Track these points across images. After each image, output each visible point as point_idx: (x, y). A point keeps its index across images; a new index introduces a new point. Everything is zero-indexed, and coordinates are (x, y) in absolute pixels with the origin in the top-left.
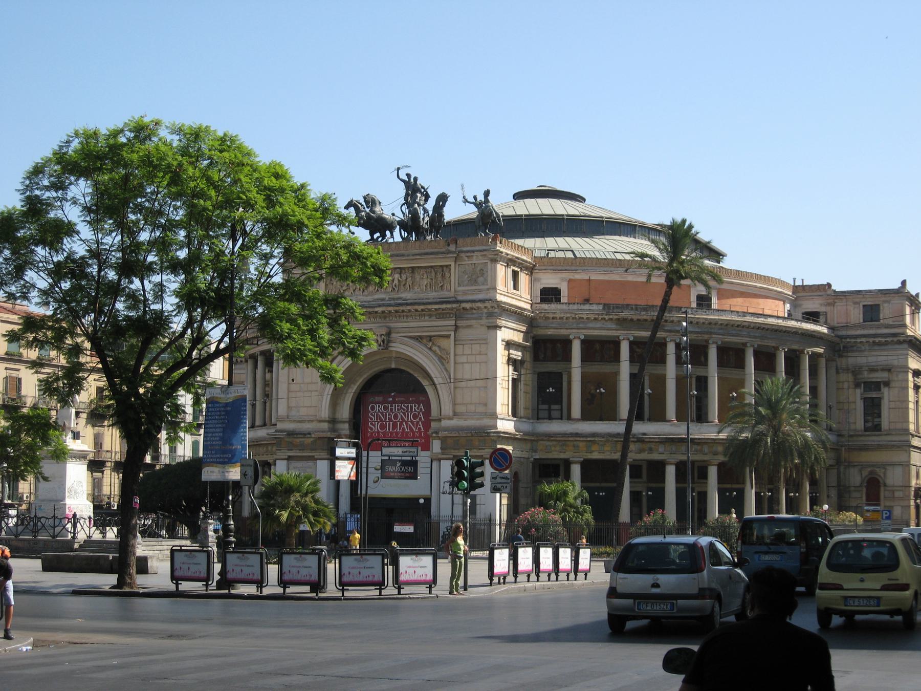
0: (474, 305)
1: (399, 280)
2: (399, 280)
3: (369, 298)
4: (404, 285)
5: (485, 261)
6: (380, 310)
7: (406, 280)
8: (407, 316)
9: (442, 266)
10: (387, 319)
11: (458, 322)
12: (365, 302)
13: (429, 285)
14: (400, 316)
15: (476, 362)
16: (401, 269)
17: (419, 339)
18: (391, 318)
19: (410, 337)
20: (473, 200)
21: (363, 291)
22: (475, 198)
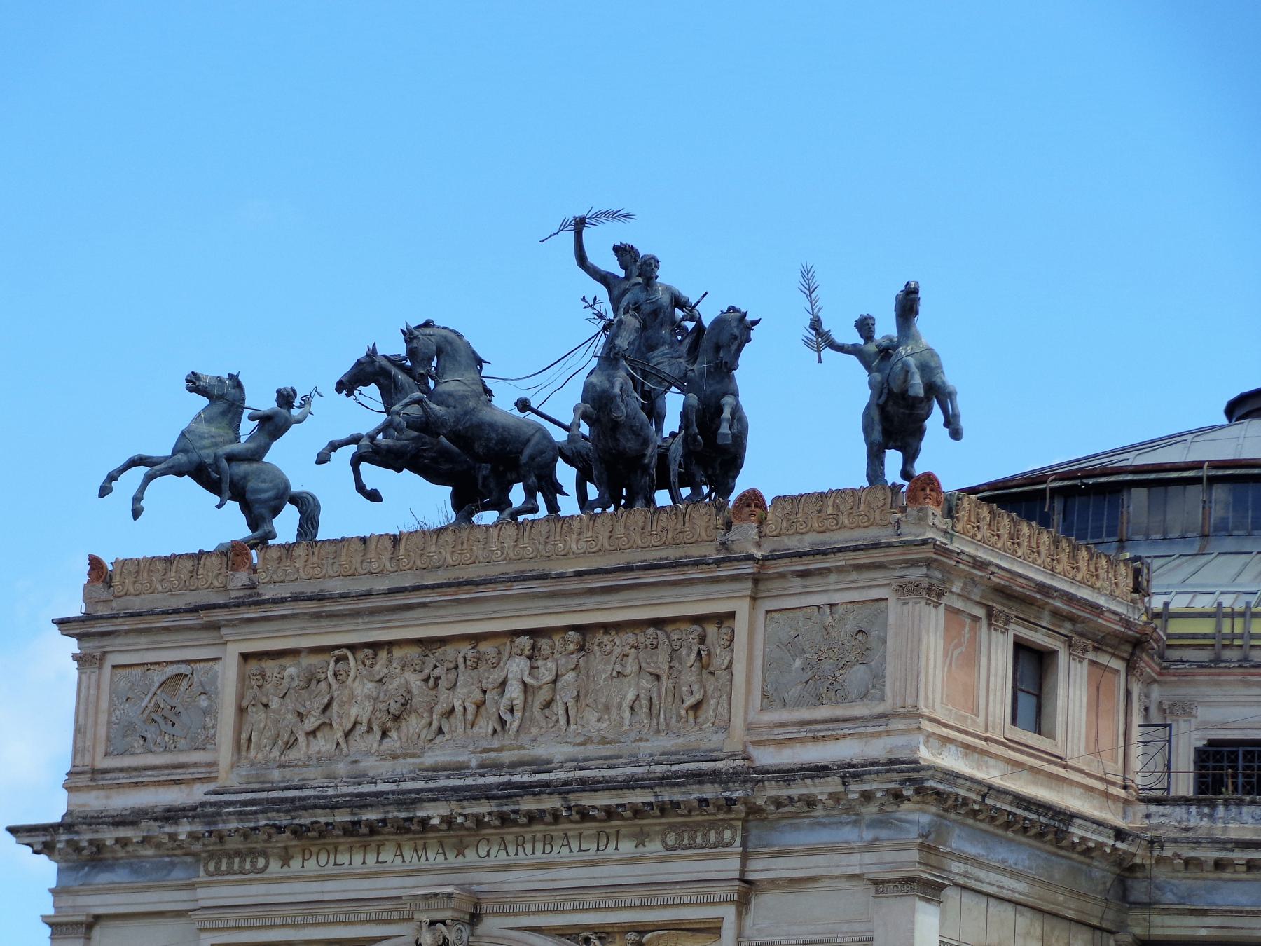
2: (524, 684)
3: (404, 766)
4: (548, 705)
7: (555, 682)
8: (548, 840)
9: (698, 620)
10: (470, 856)
11: (754, 864)
13: (645, 703)
14: (520, 843)
16: (532, 633)
18: (483, 853)
20: (855, 338)
21: (384, 734)
22: (865, 326)
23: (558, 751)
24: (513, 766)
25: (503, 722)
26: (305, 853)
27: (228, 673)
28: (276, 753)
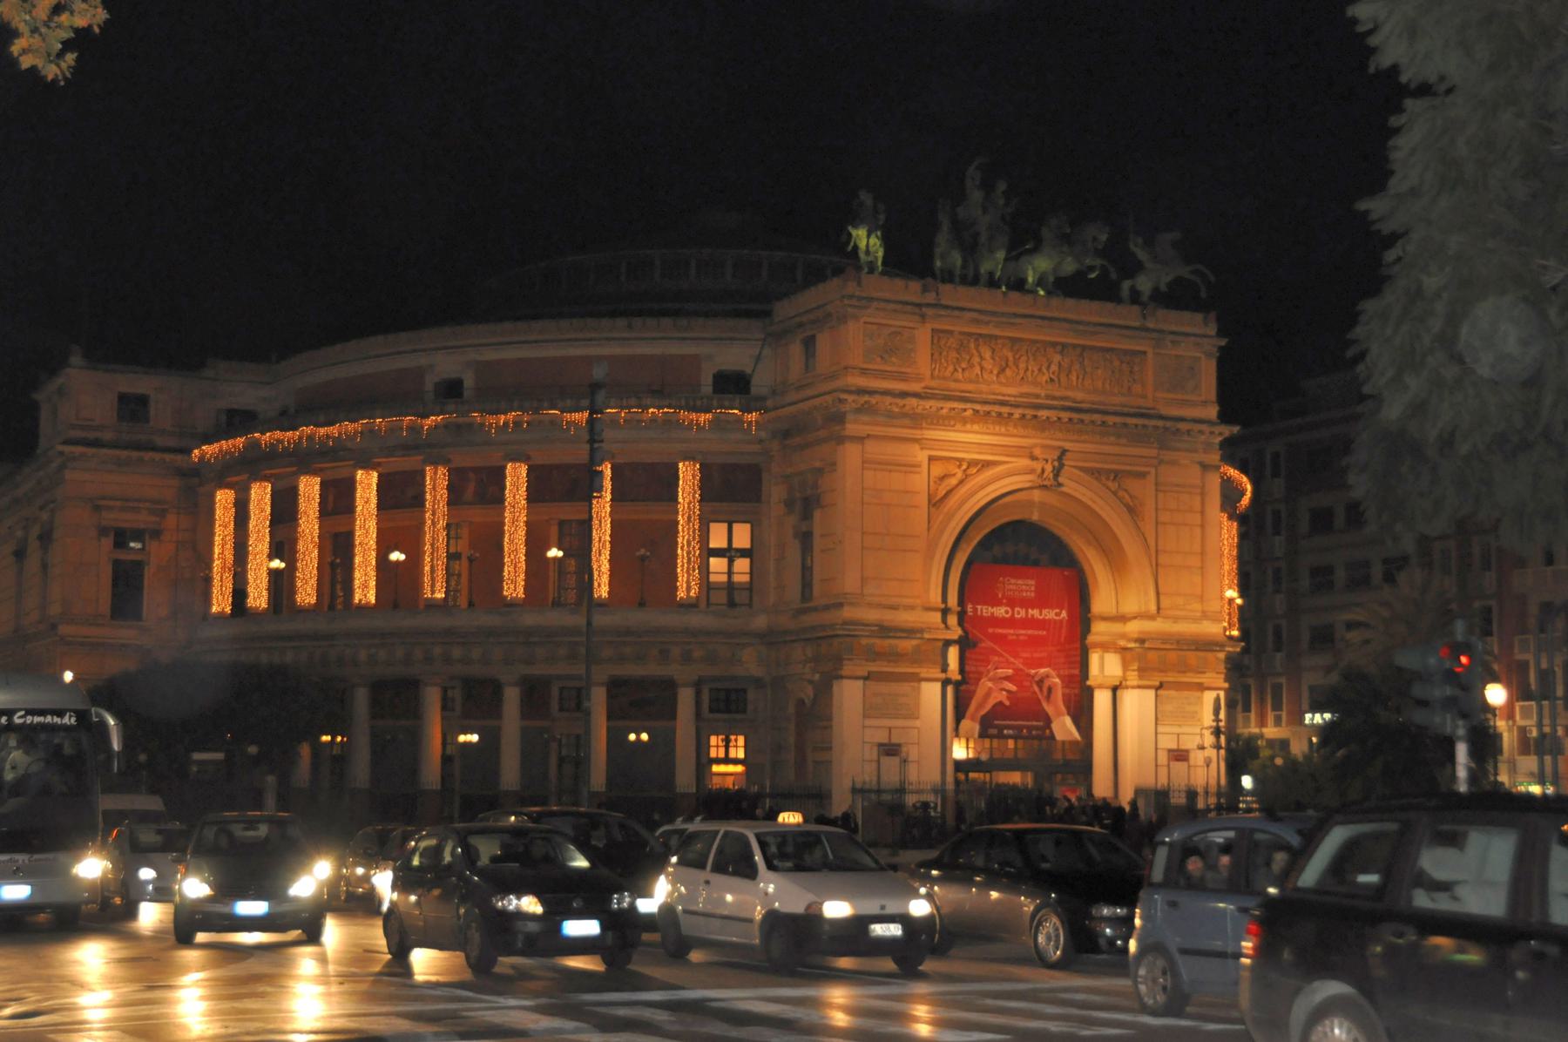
0: (1183, 426)
1: (1059, 363)
5: (1198, 355)
6: (1043, 414)
12: (1009, 396)
13: (1108, 381)
15: (1186, 525)
16: (1064, 346)
17: (1095, 473)
19: (1081, 469)
21: (998, 375)
23: (1079, 395)
24: (1062, 398)
25: (1052, 380)
26: (973, 422)
27: (923, 334)
28: (948, 374)
